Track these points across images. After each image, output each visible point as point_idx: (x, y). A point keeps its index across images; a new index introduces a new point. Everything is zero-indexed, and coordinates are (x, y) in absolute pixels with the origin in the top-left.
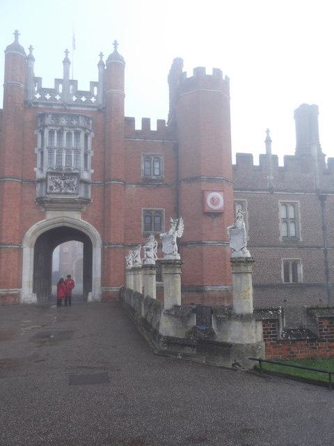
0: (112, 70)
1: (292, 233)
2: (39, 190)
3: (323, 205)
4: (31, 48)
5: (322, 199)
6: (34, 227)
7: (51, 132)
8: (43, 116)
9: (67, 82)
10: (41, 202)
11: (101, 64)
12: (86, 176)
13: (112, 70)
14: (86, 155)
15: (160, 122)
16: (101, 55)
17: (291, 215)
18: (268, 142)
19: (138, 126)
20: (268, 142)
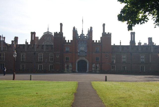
0: (90, 32)
1: (125, 61)
2: (78, 54)
3: (131, 55)
4: (77, 29)
5: (131, 54)
6: (77, 60)
7: (80, 44)
8: (79, 41)
9: (82, 35)
10: (79, 56)
11: (88, 31)
12: (86, 51)
13: (90, 32)
14: (86, 48)
15: (99, 41)
16: (88, 29)
17: (125, 57)
18: (120, 43)
19: (95, 42)
20: (120, 43)
